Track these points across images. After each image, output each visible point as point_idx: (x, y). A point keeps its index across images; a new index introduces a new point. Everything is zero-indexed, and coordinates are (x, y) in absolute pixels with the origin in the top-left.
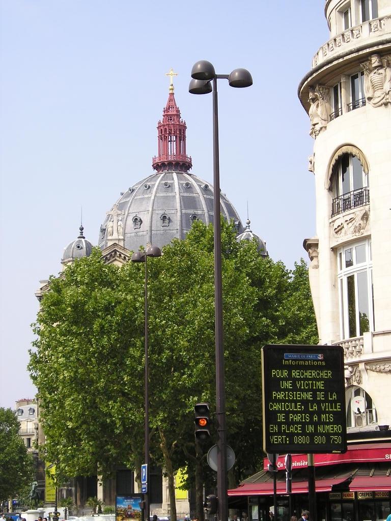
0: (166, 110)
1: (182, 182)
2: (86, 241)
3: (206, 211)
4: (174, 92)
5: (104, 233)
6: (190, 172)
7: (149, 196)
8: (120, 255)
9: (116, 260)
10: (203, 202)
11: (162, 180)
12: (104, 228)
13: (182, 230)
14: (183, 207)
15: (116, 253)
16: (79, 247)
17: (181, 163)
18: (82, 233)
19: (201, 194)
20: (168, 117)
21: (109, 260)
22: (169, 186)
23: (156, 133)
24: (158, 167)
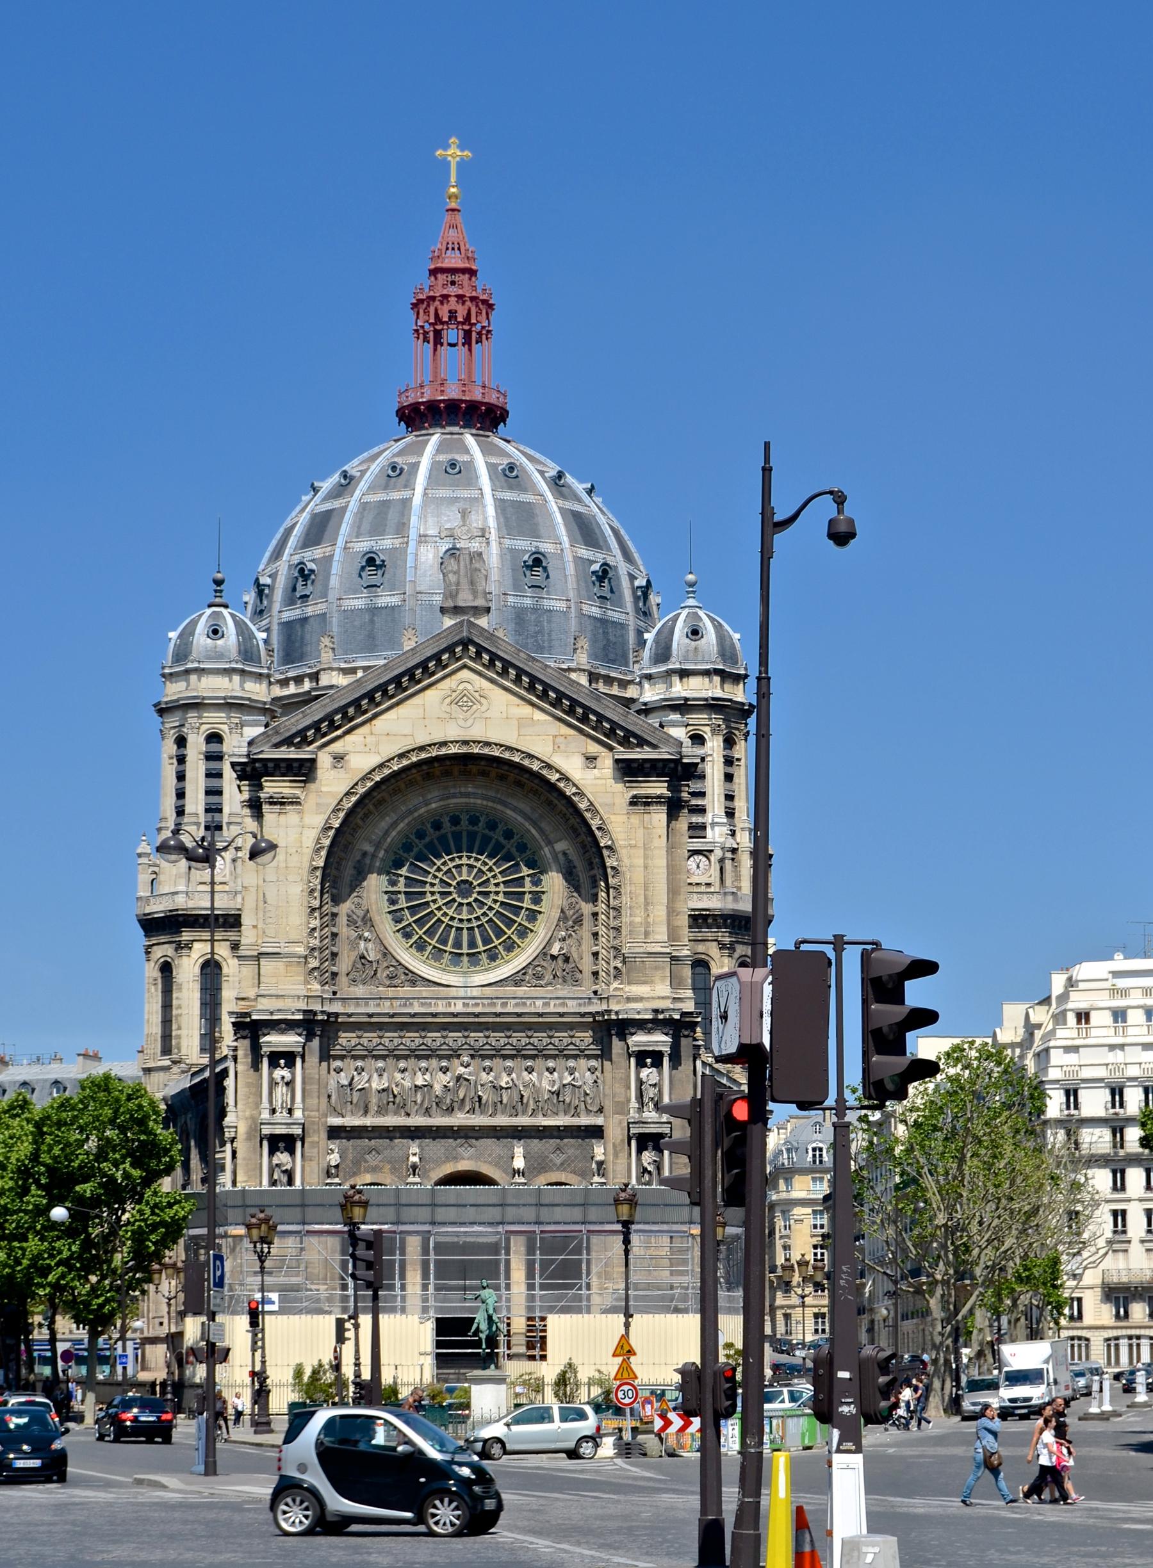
1: (494, 460)
3: (565, 540)
7: (406, 494)
9: (465, 666)
10: (559, 518)
11: (439, 451)
19: (549, 496)
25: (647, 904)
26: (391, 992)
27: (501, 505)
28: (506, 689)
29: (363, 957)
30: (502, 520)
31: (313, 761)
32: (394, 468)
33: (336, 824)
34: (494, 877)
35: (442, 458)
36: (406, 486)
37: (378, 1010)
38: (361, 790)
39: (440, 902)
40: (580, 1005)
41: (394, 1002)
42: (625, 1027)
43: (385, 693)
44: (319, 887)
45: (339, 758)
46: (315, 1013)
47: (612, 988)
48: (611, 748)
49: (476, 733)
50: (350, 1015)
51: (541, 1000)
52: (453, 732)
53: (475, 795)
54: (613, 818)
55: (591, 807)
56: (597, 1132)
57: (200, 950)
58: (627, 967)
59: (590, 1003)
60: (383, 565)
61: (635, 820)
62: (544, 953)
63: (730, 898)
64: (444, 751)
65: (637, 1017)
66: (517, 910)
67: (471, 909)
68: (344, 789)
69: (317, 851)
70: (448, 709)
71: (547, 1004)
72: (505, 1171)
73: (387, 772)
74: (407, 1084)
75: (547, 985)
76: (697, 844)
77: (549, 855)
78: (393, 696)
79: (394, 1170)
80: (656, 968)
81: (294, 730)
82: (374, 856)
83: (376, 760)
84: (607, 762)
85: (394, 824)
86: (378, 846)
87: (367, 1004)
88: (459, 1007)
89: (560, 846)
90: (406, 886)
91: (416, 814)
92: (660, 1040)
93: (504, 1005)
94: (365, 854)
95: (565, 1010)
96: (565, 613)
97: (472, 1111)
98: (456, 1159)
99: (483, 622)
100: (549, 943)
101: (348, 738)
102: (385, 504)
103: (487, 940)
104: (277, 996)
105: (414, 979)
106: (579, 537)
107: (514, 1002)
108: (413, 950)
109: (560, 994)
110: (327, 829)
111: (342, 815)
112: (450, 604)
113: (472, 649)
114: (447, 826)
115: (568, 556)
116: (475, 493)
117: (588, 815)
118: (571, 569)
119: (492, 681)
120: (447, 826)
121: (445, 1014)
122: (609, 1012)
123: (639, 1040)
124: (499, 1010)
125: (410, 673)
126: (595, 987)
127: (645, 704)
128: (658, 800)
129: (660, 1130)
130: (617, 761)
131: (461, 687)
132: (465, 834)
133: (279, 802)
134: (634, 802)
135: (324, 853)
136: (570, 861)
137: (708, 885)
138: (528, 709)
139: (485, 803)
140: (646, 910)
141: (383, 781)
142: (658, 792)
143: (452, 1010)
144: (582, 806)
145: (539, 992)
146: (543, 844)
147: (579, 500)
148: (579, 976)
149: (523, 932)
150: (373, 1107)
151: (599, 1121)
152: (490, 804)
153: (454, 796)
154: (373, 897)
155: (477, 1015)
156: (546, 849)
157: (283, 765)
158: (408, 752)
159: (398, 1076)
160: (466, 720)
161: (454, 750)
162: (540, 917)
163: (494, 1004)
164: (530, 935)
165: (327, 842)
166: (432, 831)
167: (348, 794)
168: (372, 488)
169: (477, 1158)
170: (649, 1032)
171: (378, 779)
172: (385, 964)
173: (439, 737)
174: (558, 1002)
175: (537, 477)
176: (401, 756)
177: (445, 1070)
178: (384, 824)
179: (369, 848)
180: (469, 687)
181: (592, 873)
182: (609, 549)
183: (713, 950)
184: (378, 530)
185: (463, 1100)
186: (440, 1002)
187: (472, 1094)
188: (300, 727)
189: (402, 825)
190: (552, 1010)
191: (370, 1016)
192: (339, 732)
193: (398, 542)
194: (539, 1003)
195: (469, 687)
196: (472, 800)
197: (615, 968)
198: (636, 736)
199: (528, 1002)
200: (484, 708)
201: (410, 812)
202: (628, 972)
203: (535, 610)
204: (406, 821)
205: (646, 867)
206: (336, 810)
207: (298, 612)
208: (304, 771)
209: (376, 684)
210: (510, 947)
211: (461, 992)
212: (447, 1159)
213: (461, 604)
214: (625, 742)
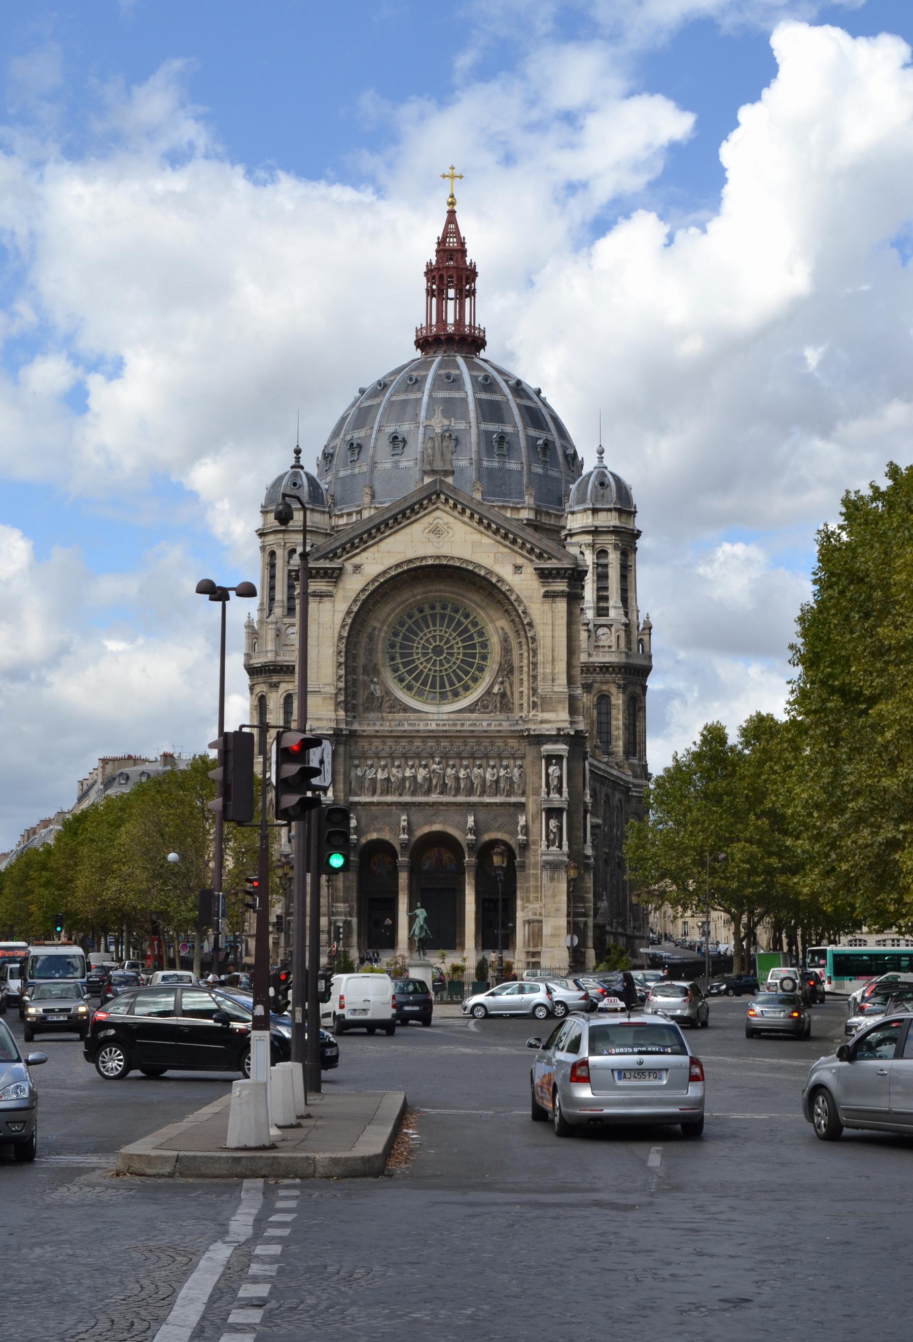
0: (442, 242)
1: (475, 373)
2: (307, 474)
3: (520, 427)
4: (456, 208)
5: (331, 461)
6: (483, 354)
7: (418, 395)
8: (447, 501)
9: (438, 508)
10: (516, 411)
11: (440, 367)
12: (331, 451)
13: (480, 460)
14: (481, 419)
16: (295, 484)
17: (470, 339)
18: (298, 459)
19: (510, 396)
20: (443, 250)
21: (425, 509)
22: (454, 381)
23: (422, 283)
24: (423, 343)
25: (553, 661)
26: (390, 716)
27: (479, 403)
28: (464, 523)
29: (372, 694)
30: (479, 412)
31: (341, 569)
32: (411, 380)
33: (355, 609)
34: (457, 643)
35: (442, 372)
36: (419, 390)
37: (382, 728)
38: (371, 588)
39: (422, 660)
40: (510, 725)
41: (392, 723)
42: (539, 739)
43: (387, 525)
44: (344, 650)
45: (357, 568)
46: (341, 730)
47: (531, 714)
48: (531, 561)
49: (445, 550)
50: (364, 731)
51: (486, 722)
53: (445, 592)
54: (532, 605)
55: (518, 599)
56: (521, 807)
57: (283, 687)
58: (541, 703)
59: (517, 724)
60: (404, 441)
61: (547, 607)
62: (488, 692)
63: (624, 655)
64: (424, 563)
65: (547, 733)
66: (471, 665)
67: (442, 665)
68: (360, 587)
69: (343, 626)
71: (490, 725)
72: (462, 831)
73: (388, 576)
74: (400, 775)
75: (490, 712)
76: (602, 620)
78: (391, 528)
79: (391, 830)
80: (560, 702)
81: (329, 549)
82: (380, 630)
83: (380, 568)
84: (529, 571)
85: (394, 609)
86: (383, 623)
87: (374, 724)
88: (433, 727)
90: (401, 648)
92: (562, 748)
93: (462, 725)
94: (374, 628)
95: (501, 728)
96: (520, 472)
97: (441, 793)
98: (431, 823)
99: (450, 480)
100: (492, 686)
101: (364, 555)
102: (405, 402)
103: (452, 684)
104: (318, 719)
105: (406, 709)
106: (529, 422)
107: (468, 723)
108: (405, 690)
109: (499, 718)
110: (348, 613)
111: (359, 603)
112: (428, 468)
113: (443, 497)
114: (427, 611)
115: (522, 435)
116: (462, 395)
117: (516, 604)
118: (523, 442)
119: (455, 518)
120: (427, 611)
121: (424, 731)
122: (528, 730)
123: (548, 748)
124: (459, 728)
125: (403, 513)
126: (521, 714)
127: (570, 530)
128: (561, 594)
129: (561, 806)
130: (536, 569)
131: (435, 522)
132: (438, 616)
133: (320, 595)
134: (546, 595)
135: (347, 628)
136: (506, 634)
137: (610, 647)
138: (477, 537)
140: (553, 664)
141: (385, 582)
142: (561, 588)
143: (429, 728)
144: (513, 598)
145: (486, 716)
147: (530, 398)
148: (511, 706)
149: (475, 680)
150: (379, 791)
151: (523, 800)
153: (431, 592)
154: (380, 656)
155: (446, 731)
156: (490, 625)
157: (322, 571)
158: (402, 563)
159: (394, 770)
160: (439, 543)
161: (430, 562)
162: (486, 669)
163: (455, 725)
164: (480, 681)
165: (349, 621)
166: (417, 613)
167: (363, 590)
168: (396, 392)
169: (444, 823)
170: (556, 742)
171: (382, 580)
172: (387, 699)
173: (420, 553)
174: (497, 723)
175: (503, 385)
176: (397, 566)
177: (426, 766)
178: (387, 609)
179: (378, 625)
180: (441, 522)
181: (519, 640)
182: (550, 431)
183: (613, 690)
184: (400, 420)
185: (436, 786)
186: (421, 723)
188: (333, 547)
189: (398, 610)
190: (493, 728)
191: (377, 731)
192: (357, 551)
193: (412, 426)
194: (485, 724)
195: (441, 522)
197: (533, 702)
198: (547, 553)
199: (478, 723)
200: (450, 535)
201: (404, 602)
202: (541, 705)
203: (500, 469)
204: (401, 607)
205: (553, 637)
206: (355, 601)
207: (349, 472)
208: (335, 576)
209: (382, 519)
210: (467, 688)
211: (436, 717)
212: (426, 824)
213: (436, 469)
214: (540, 556)
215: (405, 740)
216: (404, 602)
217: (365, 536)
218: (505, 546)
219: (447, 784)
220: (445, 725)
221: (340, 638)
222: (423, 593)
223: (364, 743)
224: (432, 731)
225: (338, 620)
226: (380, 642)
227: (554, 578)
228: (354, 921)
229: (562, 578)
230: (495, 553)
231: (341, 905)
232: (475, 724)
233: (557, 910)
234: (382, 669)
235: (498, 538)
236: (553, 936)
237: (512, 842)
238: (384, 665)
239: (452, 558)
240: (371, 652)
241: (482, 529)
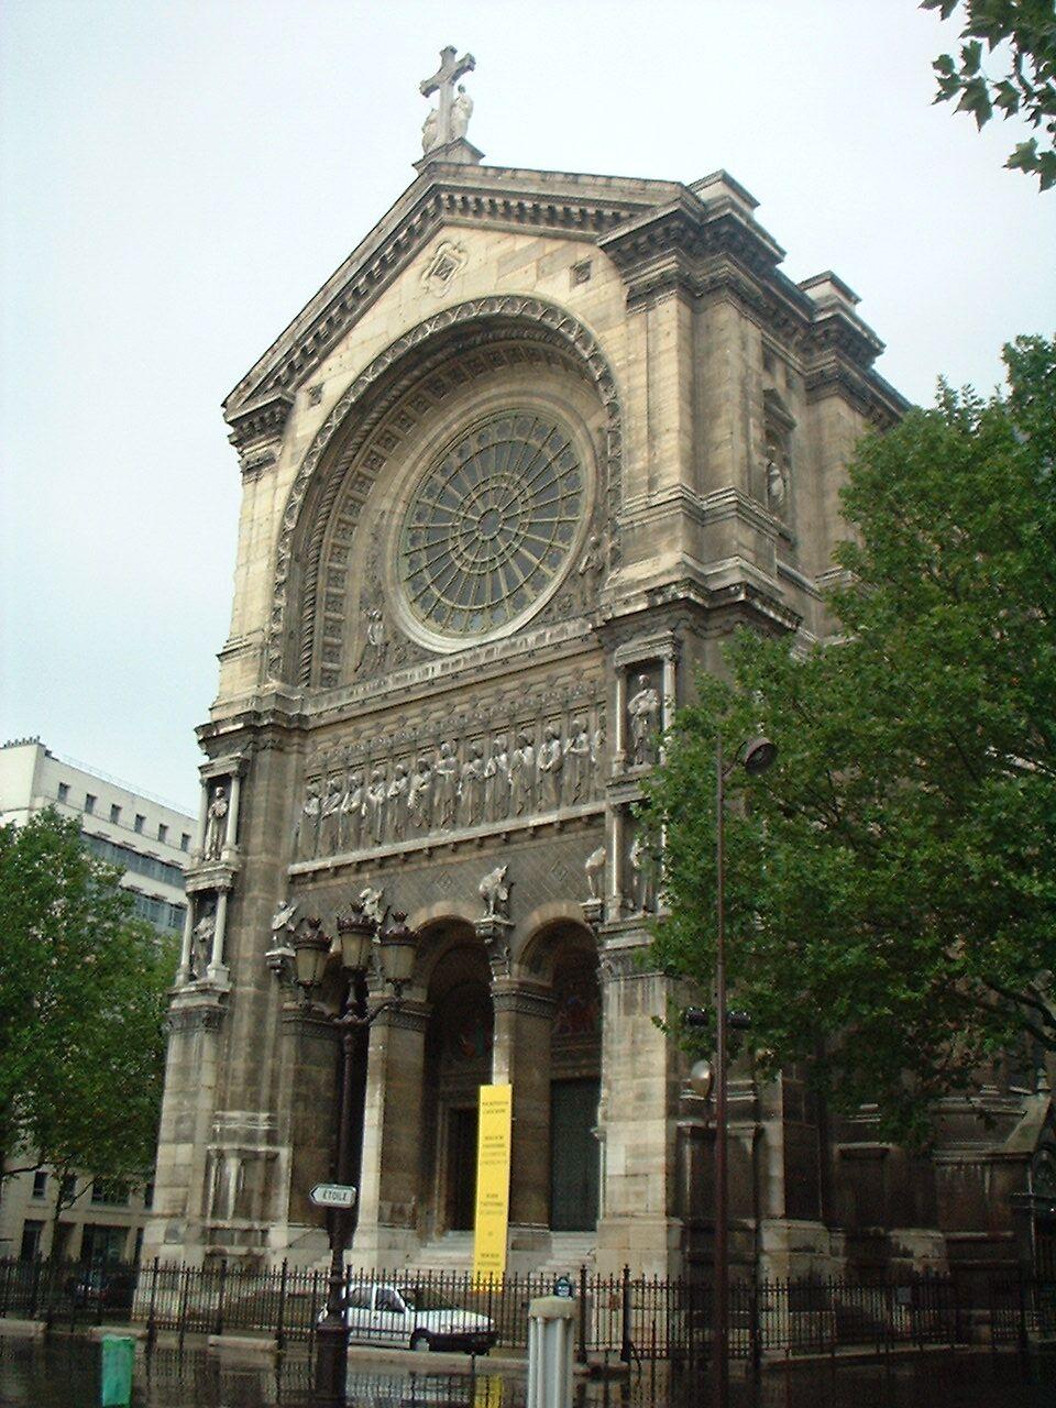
9: (442, 225)
15: (438, 201)
38: (336, 422)
45: (316, 394)
52: (428, 309)
54: (607, 335)
65: (627, 611)
69: (288, 512)
70: (424, 283)
71: (542, 637)
77: (582, 439)
80: (662, 530)
83: (349, 377)
85: (415, 465)
86: (396, 500)
89: (592, 424)
91: (436, 445)
93: (490, 652)
98: (429, 900)
101: (326, 364)
110: (298, 481)
128: (664, 283)
139: (510, 400)
140: (651, 447)
146: (574, 427)
152: (516, 400)
153: (475, 406)
156: (578, 432)
157: (256, 419)
158: (382, 354)
163: (477, 656)
165: (299, 498)
173: (412, 322)
176: (377, 361)
178: (403, 471)
179: (386, 505)
187: (448, 796)
191: (341, 710)
196: (495, 403)
204: (427, 457)
206: (310, 455)
215: (393, 718)
216: (430, 445)
217: (322, 326)
218: (556, 237)
219: (457, 799)
220: (458, 662)
221: (284, 533)
222: (461, 416)
223: (324, 742)
224: (431, 683)
225: (280, 505)
226: (391, 537)
227: (647, 254)
228: (285, 1153)
229: (663, 247)
230: (538, 260)
231: (236, 1114)
232: (514, 645)
233: (641, 1097)
234: (391, 589)
235: (543, 227)
236: (631, 1175)
237: (579, 916)
238: (396, 581)
239: (465, 305)
240: (374, 561)
241: (514, 224)
